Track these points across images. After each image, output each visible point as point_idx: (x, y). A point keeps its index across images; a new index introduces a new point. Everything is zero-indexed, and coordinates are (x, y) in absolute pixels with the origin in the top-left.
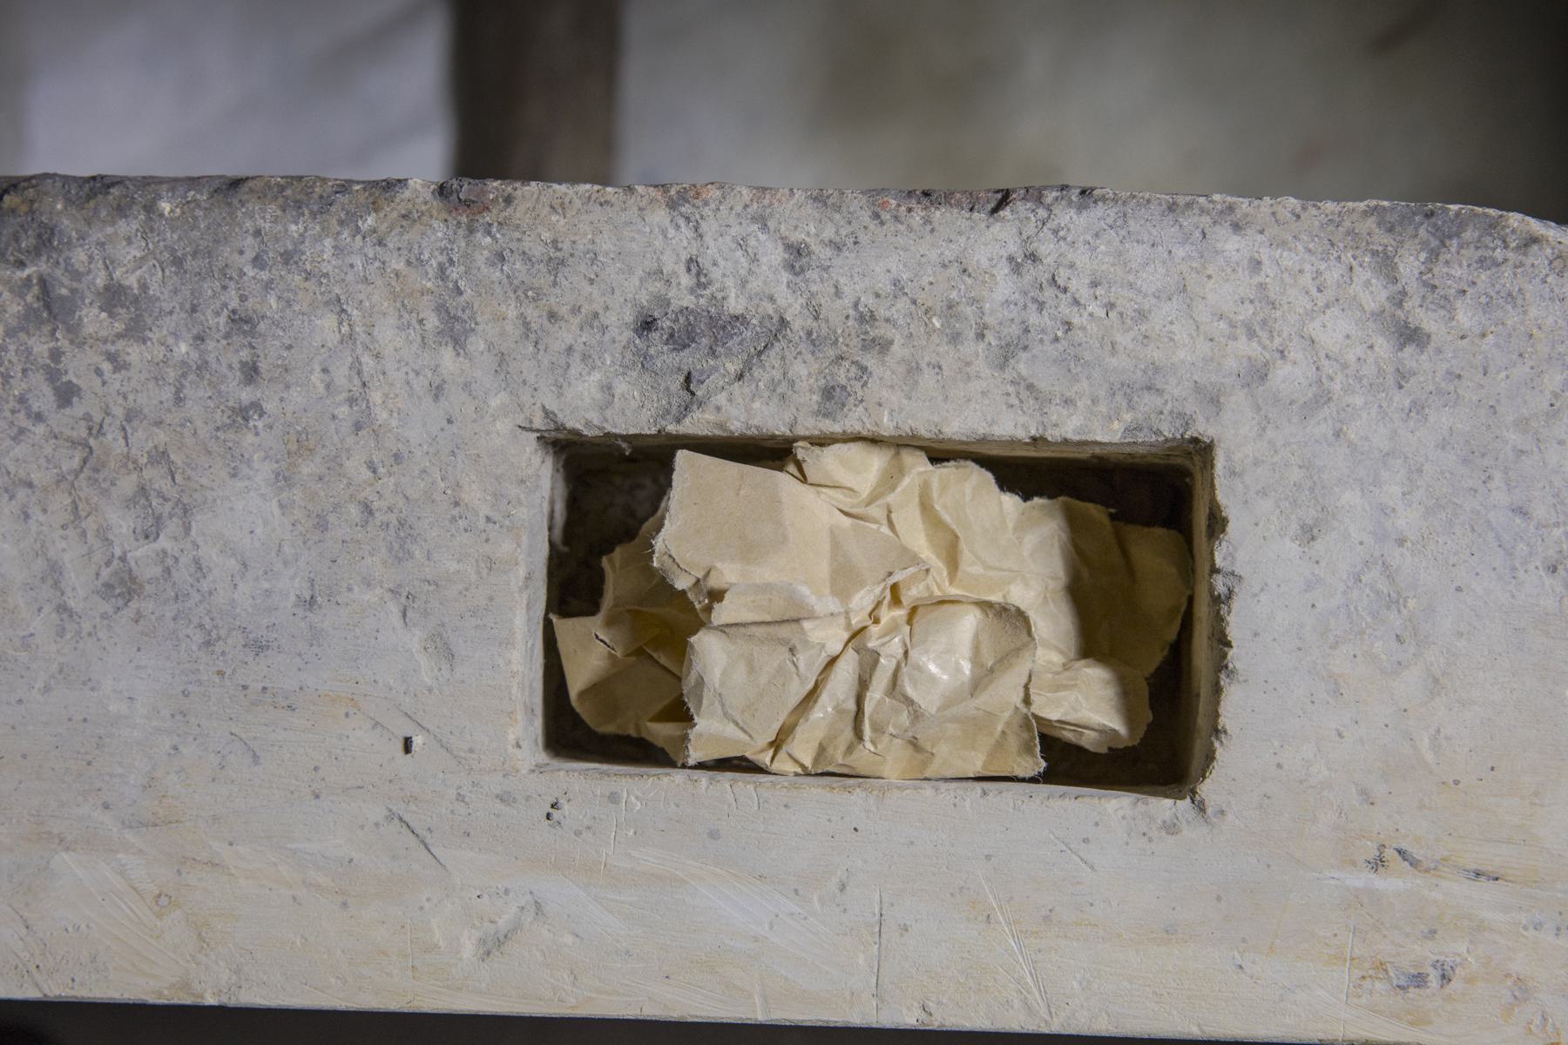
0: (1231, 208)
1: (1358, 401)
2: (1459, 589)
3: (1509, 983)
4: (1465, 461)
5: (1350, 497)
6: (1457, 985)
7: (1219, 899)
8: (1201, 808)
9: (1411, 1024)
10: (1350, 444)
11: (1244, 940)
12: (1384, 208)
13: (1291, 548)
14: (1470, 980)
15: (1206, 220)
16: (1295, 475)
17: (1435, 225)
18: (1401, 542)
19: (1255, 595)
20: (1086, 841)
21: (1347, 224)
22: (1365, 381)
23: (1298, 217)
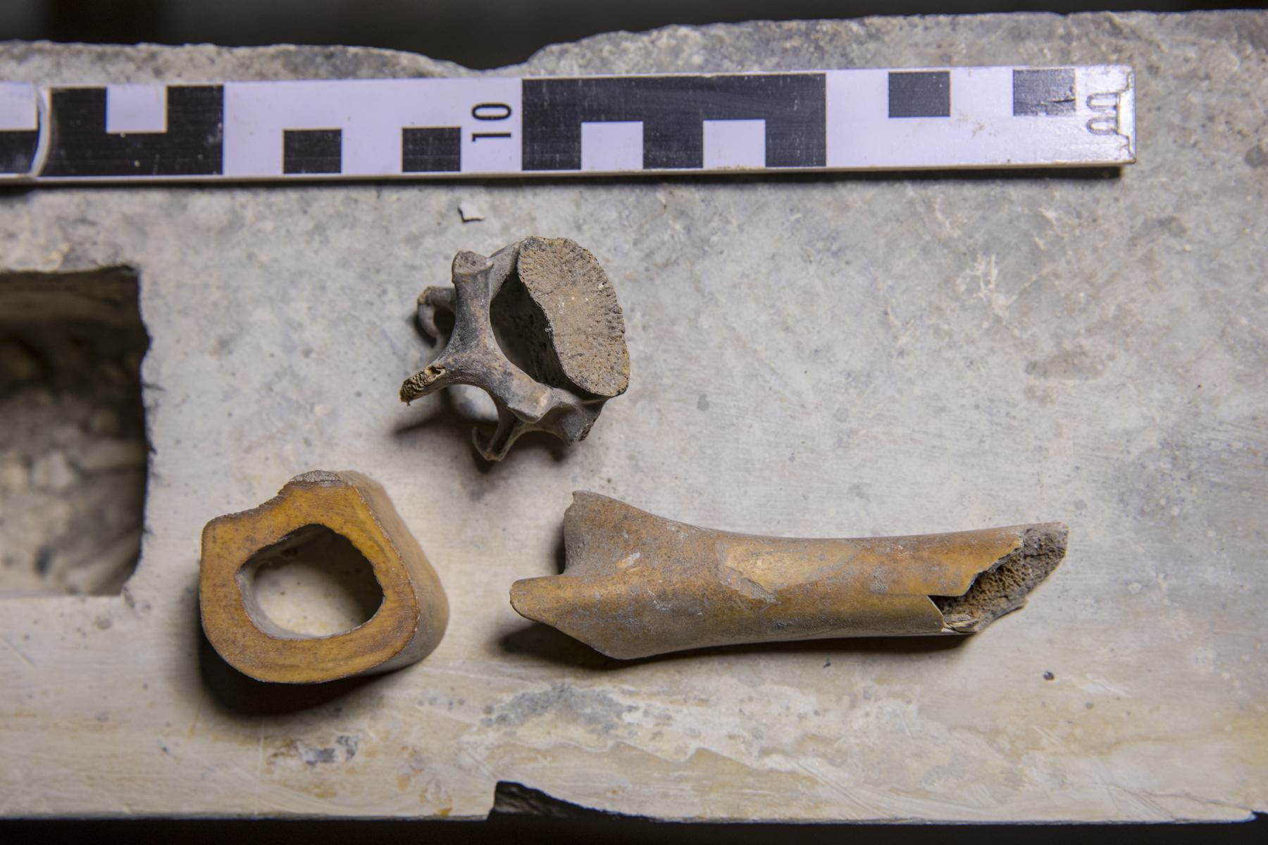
0: (153, 56)
1: (268, 226)
2: (359, 394)
3: (406, 754)
4: (363, 277)
5: (262, 314)
6: (359, 758)
7: (146, 687)
8: (130, 602)
9: (320, 796)
10: (262, 266)
11: (168, 725)
12: (289, 52)
13: (211, 362)
14: (371, 754)
15: (131, 67)
16: (215, 295)
17: (335, 67)
18: (307, 353)
19: (177, 406)
20: (27, 637)
21: (257, 66)
22: (274, 208)
23: (212, 61)
